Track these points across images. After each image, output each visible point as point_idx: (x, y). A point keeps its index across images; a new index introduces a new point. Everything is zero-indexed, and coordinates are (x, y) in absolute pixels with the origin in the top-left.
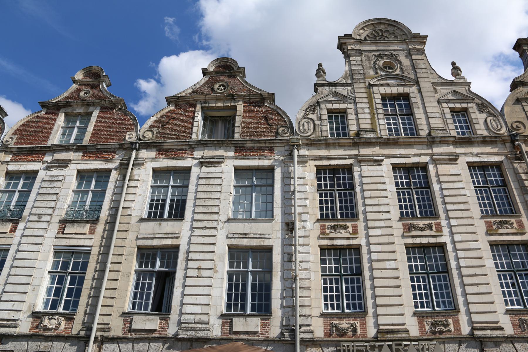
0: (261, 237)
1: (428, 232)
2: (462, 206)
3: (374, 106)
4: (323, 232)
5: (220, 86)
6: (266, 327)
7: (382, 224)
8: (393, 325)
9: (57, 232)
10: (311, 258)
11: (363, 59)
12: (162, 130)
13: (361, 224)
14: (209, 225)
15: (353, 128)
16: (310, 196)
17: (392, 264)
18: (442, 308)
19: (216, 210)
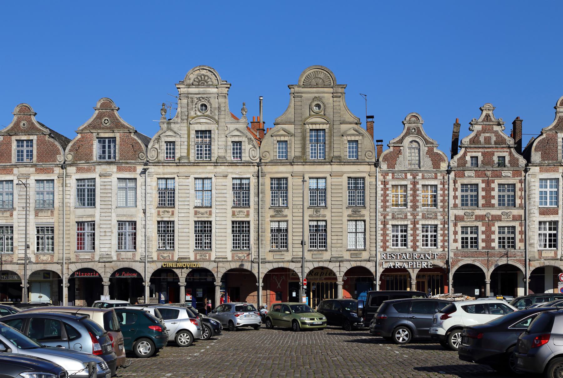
0: (131, 216)
1: (205, 215)
2: (223, 203)
3: (191, 139)
4: (159, 214)
5: (105, 120)
6: (134, 255)
7: (185, 211)
8: (184, 256)
9: (34, 215)
10: (153, 226)
11: (189, 101)
12: (76, 153)
13: (176, 210)
14: (108, 211)
15: (177, 156)
16: (154, 196)
17: (187, 230)
18: (207, 249)
19: (110, 203)
